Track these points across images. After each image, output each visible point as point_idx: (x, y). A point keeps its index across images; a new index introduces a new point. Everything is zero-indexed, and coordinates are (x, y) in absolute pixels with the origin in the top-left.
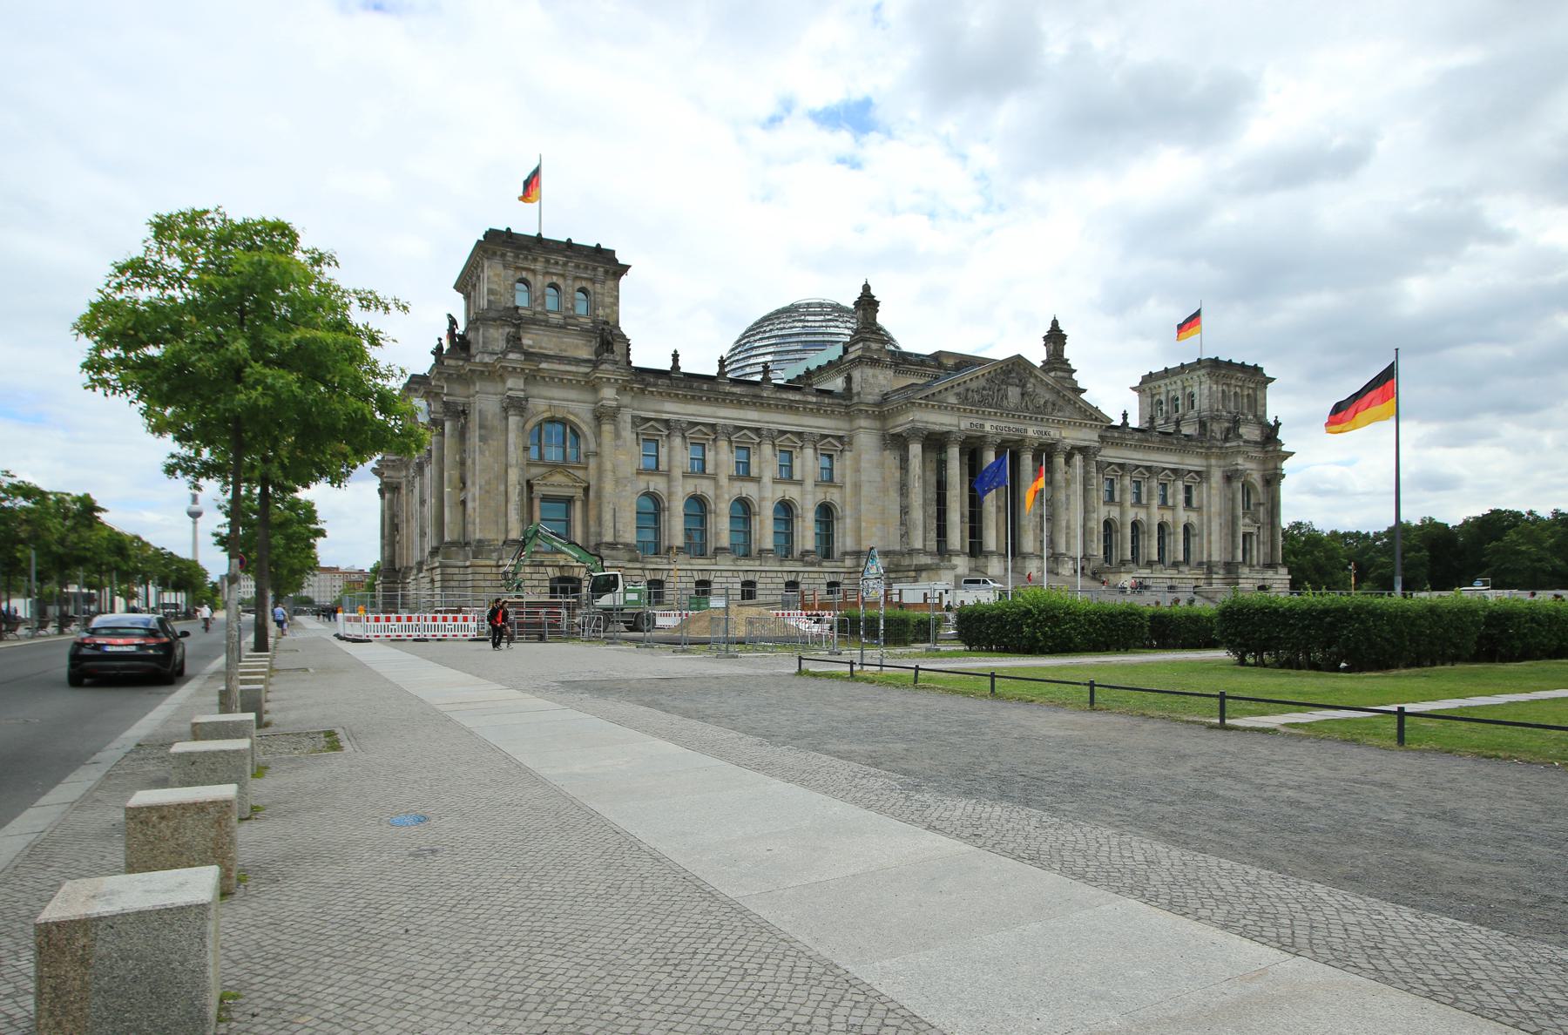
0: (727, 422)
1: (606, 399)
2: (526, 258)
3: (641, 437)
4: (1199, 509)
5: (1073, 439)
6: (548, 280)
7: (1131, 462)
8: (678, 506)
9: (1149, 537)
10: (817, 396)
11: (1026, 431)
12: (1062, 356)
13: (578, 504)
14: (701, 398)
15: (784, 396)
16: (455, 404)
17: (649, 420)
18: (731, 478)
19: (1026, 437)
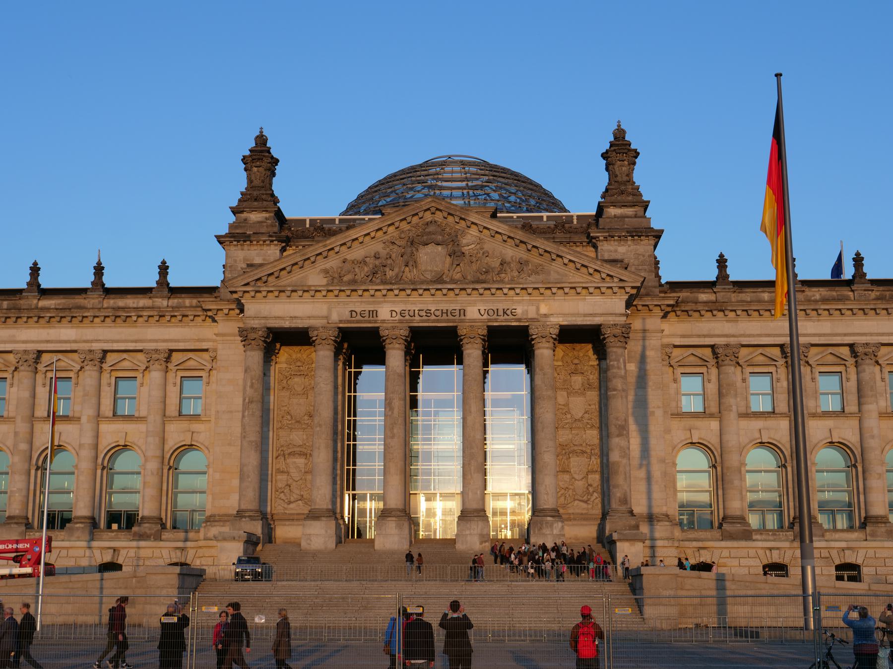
5: (564, 315)
10: (169, 298)
11: (463, 312)
12: (630, 181)
15: (121, 302)
19: (462, 321)
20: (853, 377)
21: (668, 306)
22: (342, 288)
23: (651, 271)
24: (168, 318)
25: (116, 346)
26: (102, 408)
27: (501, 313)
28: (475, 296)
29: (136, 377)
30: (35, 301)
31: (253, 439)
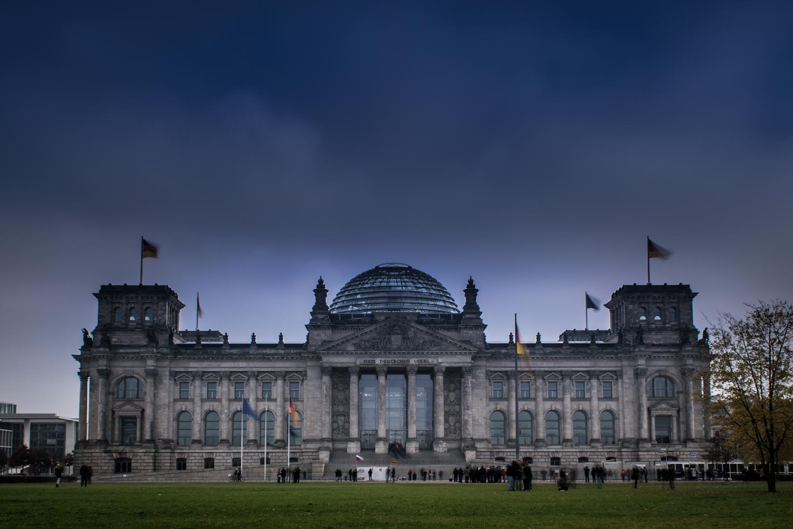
0: (227, 370)
1: (147, 366)
2: (117, 298)
3: (178, 382)
4: (617, 399)
5: (447, 363)
6: (129, 306)
7: (541, 369)
8: (198, 418)
9: (564, 421)
11: (408, 361)
13: (138, 420)
14: (208, 358)
15: (264, 351)
16: (84, 372)
17: (183, 372)
18: (230, 400)
19: (408, 365)
20: (562, 384)
21: (488, 356)
22: (362, 352)
23: (482, 342)
24: (285, 359)
25: (263, 370)
26: (258, 395)
27: (423, 361)
28: (413, 355)
29: (271, 383)
30: (228, 351)
31: (327, 410)
